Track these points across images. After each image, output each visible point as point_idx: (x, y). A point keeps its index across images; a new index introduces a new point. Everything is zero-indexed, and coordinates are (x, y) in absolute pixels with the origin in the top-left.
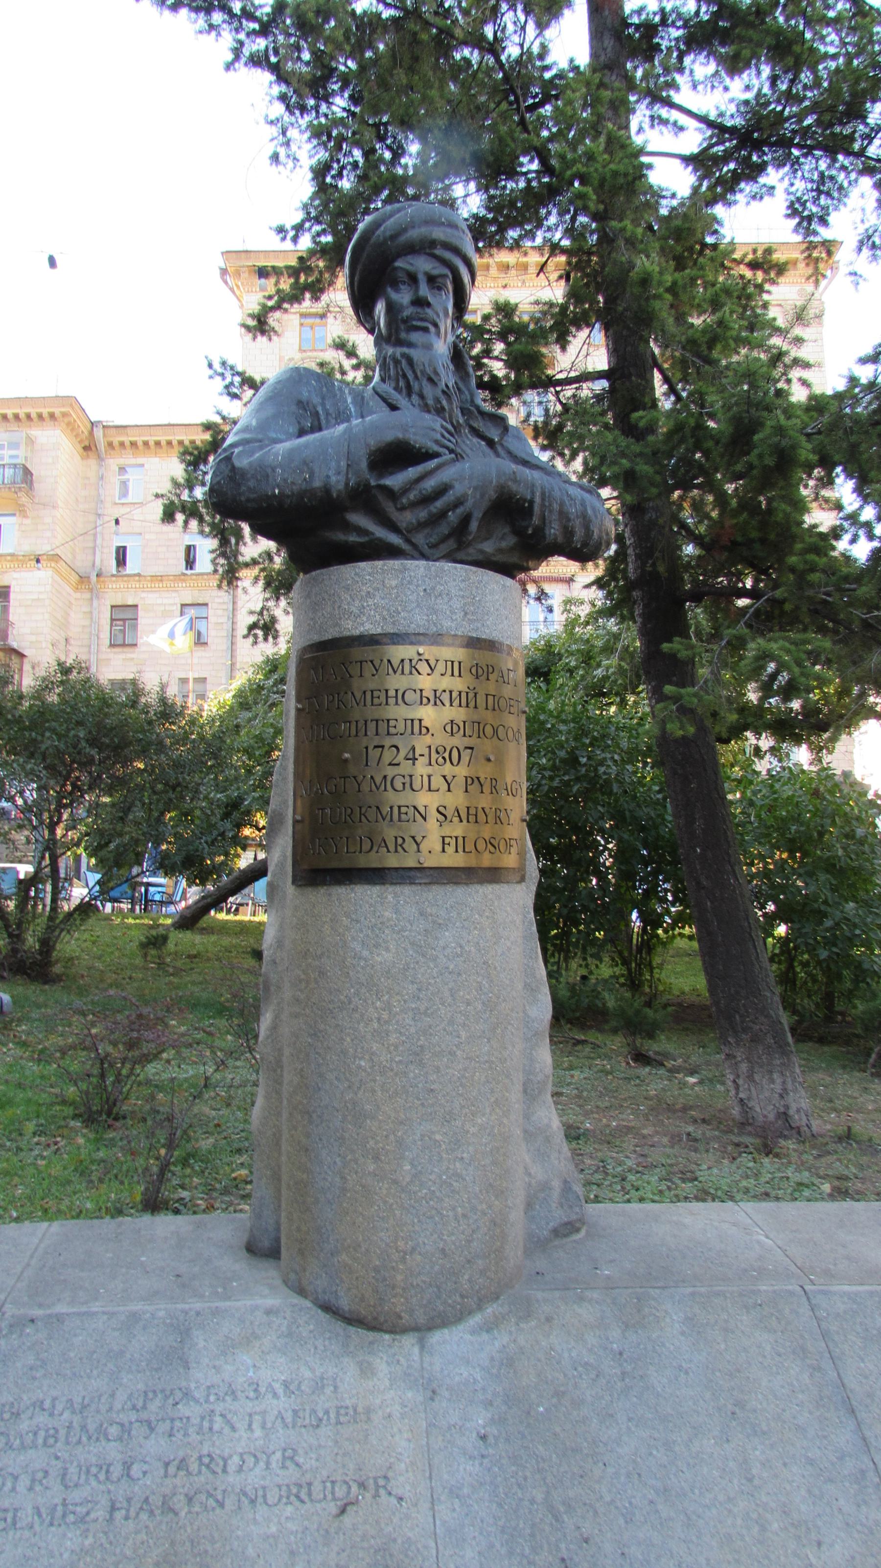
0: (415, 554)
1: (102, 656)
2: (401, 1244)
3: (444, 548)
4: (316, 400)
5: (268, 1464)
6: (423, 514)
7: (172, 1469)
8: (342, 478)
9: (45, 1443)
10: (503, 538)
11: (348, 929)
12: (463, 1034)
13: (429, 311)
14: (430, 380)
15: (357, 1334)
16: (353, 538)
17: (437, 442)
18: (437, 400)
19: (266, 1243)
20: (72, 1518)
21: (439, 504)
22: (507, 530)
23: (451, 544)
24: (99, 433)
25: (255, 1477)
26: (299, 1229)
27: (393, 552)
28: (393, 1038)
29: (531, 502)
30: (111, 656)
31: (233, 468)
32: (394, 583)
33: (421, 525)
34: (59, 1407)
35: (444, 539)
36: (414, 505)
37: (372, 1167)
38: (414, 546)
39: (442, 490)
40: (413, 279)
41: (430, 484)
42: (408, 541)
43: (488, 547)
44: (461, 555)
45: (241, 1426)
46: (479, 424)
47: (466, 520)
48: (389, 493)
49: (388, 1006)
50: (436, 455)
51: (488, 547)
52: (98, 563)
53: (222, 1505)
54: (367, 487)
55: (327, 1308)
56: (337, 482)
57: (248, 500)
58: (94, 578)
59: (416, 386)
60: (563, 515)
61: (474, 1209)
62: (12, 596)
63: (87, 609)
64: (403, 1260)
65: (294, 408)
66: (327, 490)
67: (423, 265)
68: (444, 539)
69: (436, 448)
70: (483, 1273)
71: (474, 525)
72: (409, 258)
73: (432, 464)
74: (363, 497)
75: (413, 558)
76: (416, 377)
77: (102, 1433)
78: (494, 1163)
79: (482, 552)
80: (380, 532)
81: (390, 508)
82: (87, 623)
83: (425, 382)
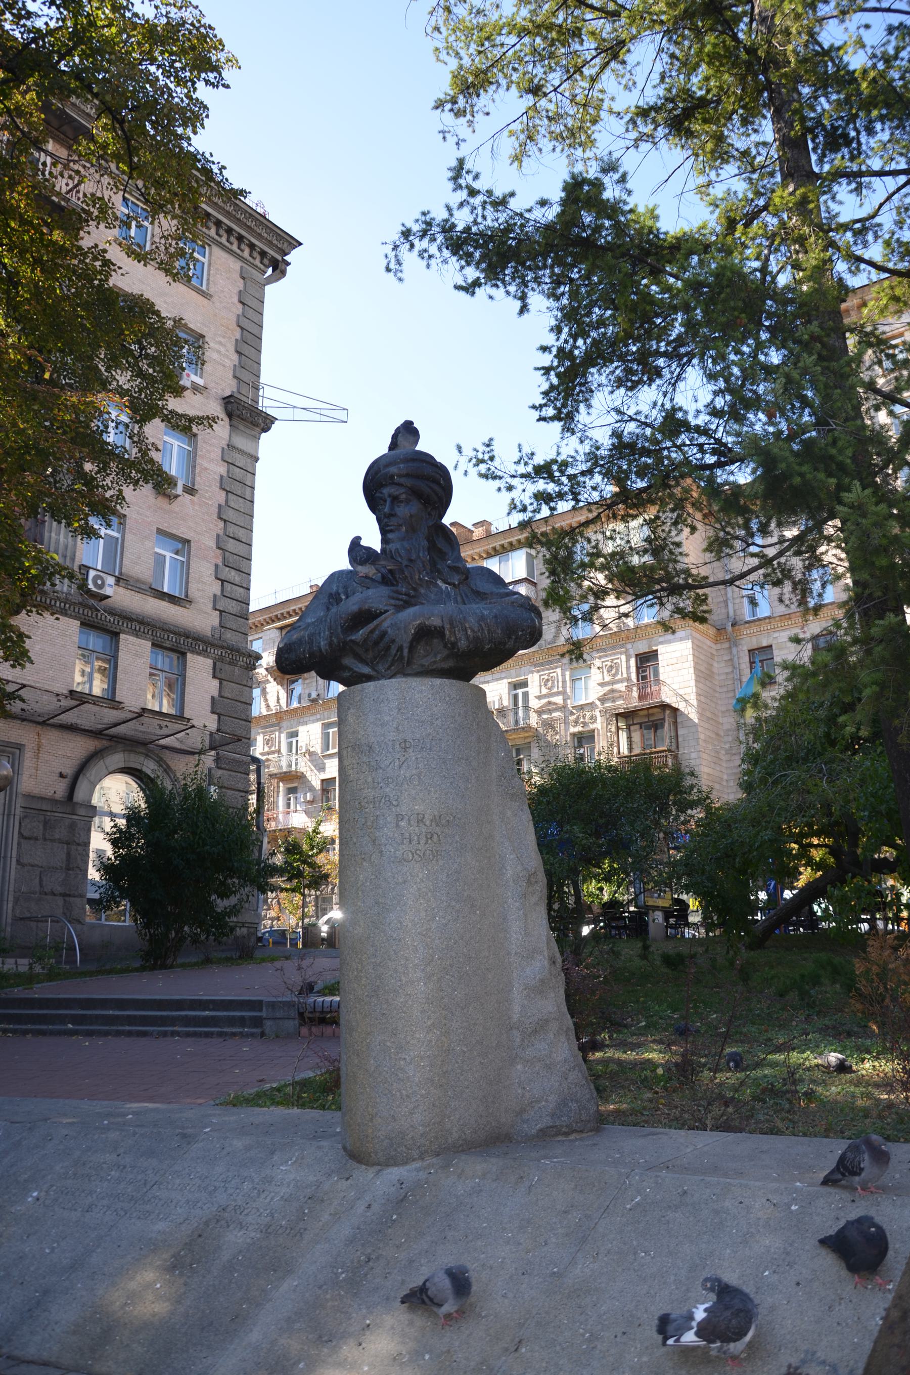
2: (370, 1109)
27: (369, 678)
41: (376, 635)
42: (374, 669)
43: (426, 662)
50: (386, 611)
52: (731, 613)
54: (345, 643)
58: (730, 628)
62: (660, 657)
63: (727, 658)
74: (345, 648)
79: (423, 666)
82: (729, 670)
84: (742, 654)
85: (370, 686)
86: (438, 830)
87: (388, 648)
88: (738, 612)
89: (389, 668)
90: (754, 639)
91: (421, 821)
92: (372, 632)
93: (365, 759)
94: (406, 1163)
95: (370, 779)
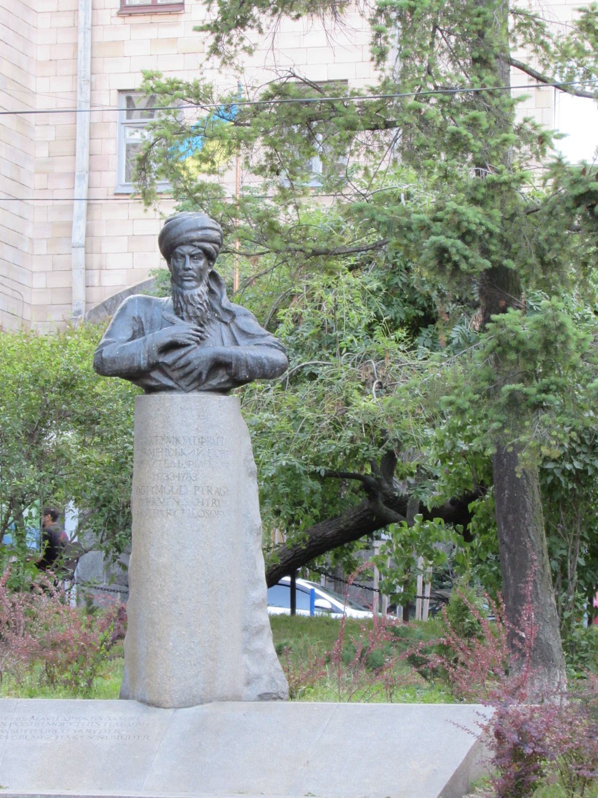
1: (102, 36)
2: (168, 674)
3: (193, 386)
4: (142, 315)
6: (181, 373)
8: (146, 361)
10: (222, 377)
12: (195, 592)
13: (190, 272)
15: (151, 709)
16: (153, 383)
17: (189, 339)
18: (195, 313)
21: (187, 369)
23: (196, 384)
28: (166, 592)
29: (231, 363)
40: (183, 256)
41: (182, 362)
43: (214, 382)
44: (202, 387)
47: (200, 374)
50: (189, 345)
51: (214, 382)
54: (158, 363)
56: (143, 363)
59: (184, 308)
65: (131, 322)
66: (139, 367)
67: (187, 249)
68: (192, 383)
70: (203, 689)
71: (204, 377)
72: (182, 247)
81: (168, 371)
86: (219, 498)
87: (191, 372)
89: (189, 385)
91: (209, 491)
92: (180, 358)
93: (173, 447)
94: (192, 706)
95: (176, 461)
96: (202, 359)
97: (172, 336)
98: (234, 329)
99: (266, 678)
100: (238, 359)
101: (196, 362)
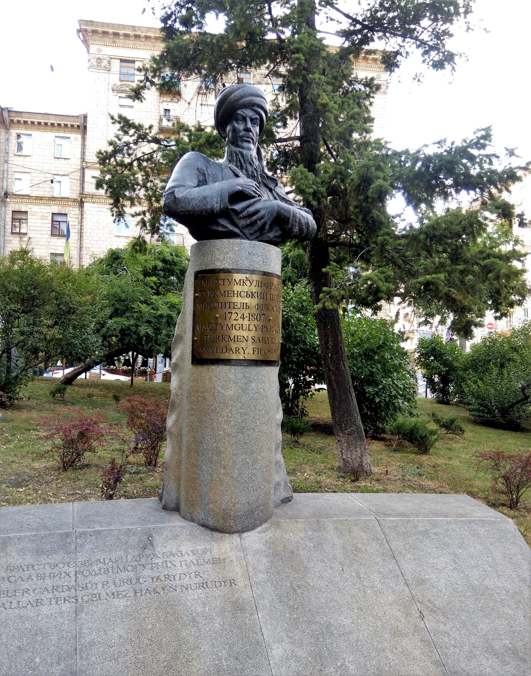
0: (244, 237)
5: (190, 577)
6: (248, 222)
7: (155, 580)
8: (218, 205)
9: (104, 573)
10: (276, 232)
11: (216, 382)
12: (258, 422)
14: (250, 164)
15: (216, 535)
16: (220, 229)
17: (254, 191)
18: (253, 172)
19: (172, 505)
20: (121, 596)
21: (255, 218)
22: (278, 228)
23: (258, 234)
24: (5, 114)
25: (186, 581)
26: (192, 497)
28: (232, 423)
29: (289, 218)
30: (12, 238)
31: (175, 197)
32: (237, 249)
33: (247, 226)
34: (107, 561)
35: (256, 232)
36: (245, 217)
37: (223, 472)
38: (244, 234)
39: (256, 212)
41: (252, 209)
42: (242, 231)
43: (271, 235)
45: (178, 565)
46: (267, 182)
47: (265, 224)
48: (235, 211)
49: (231, 411)
50: (254, 197)
51: (271, 235)
53: (176, 590)
55: (203, 526)
57: (181, 211)
60: (300, 223)
61: (260, 487)
64: (234, 506)
69: (253, 194)
71: (267, 227)
73: (253, 200)
75: (243, 239)
76: (245, 162)
77: (125, 569)
78: (267, 471)
79: (269, 237)
80: (231, 227)
83: (248, 165)
84: (8, 212)
85: (238, 241)
88: (9, 187)
89: (251, 234)
90: (17, 205)
96: (269, 210)
97: (241, 185)
98: (275, 195)
99: (283, 483)
100: (294, 216)
101: (263, 212)
